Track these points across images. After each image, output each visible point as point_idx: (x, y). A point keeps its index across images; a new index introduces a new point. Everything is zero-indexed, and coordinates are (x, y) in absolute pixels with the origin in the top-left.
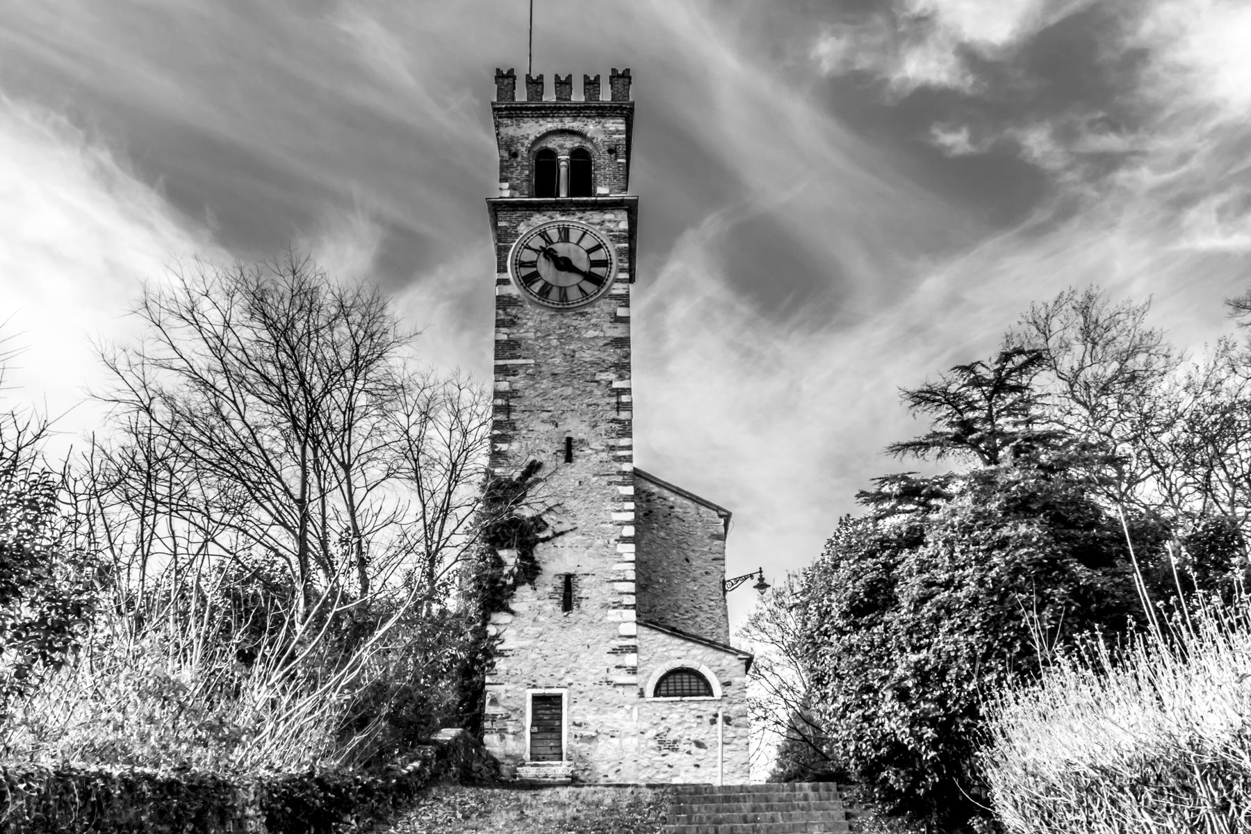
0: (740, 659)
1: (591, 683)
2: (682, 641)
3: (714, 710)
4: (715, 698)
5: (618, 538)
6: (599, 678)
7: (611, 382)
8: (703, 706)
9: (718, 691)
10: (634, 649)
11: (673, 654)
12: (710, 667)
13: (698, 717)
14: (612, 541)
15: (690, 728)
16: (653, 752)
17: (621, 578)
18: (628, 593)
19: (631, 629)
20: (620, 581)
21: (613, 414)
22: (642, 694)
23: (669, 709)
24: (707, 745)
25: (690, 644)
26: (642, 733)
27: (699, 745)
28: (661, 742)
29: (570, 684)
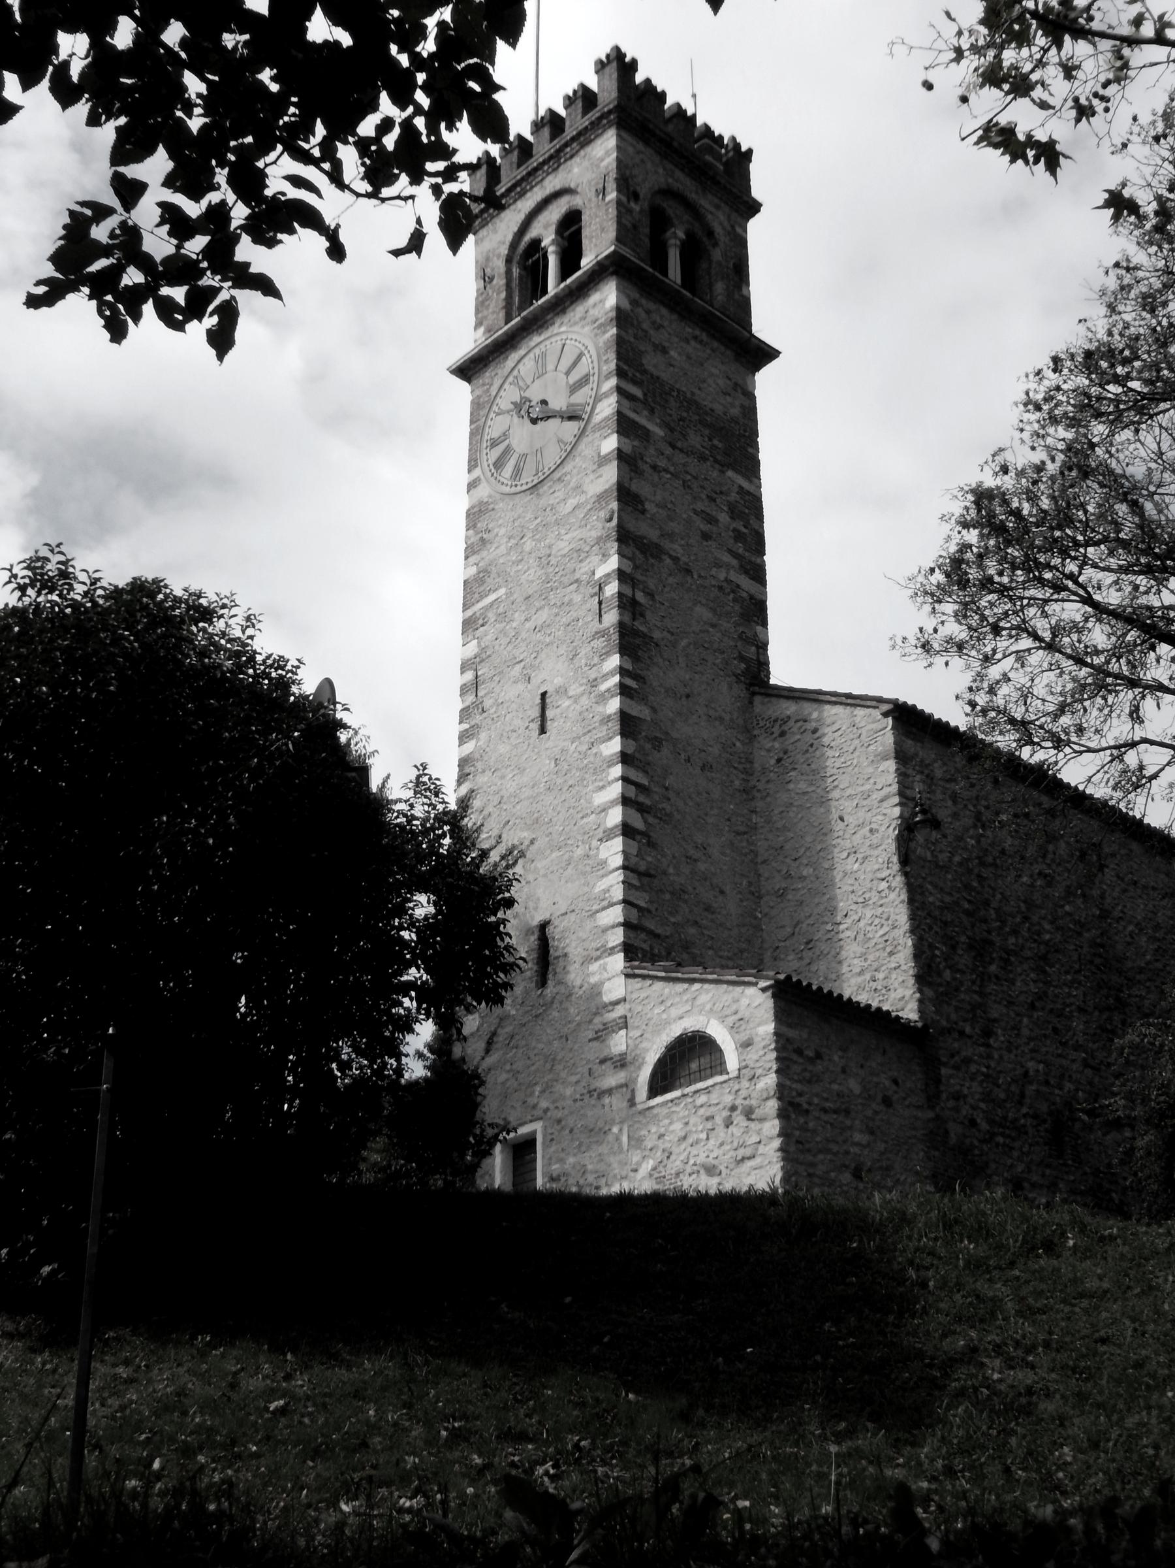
0: (764, 990)
1: (570, 1102)
2: (686, 986)
3: (728, 1099)
4: (731, 1076)
5: (601, 835)
6: (580, 1089)
8: (714, 1098)
9: (732, 1061)
11: (674, 1012)
12: (722, 1019)
13: (707, 1119)
14: (595, 843)
15: (697, 1142)
17: (605, 903)
18: (613, 927)
20: (604, 909)
24: (722, 1168)
25: (697, 986)
29: (546, 1110)
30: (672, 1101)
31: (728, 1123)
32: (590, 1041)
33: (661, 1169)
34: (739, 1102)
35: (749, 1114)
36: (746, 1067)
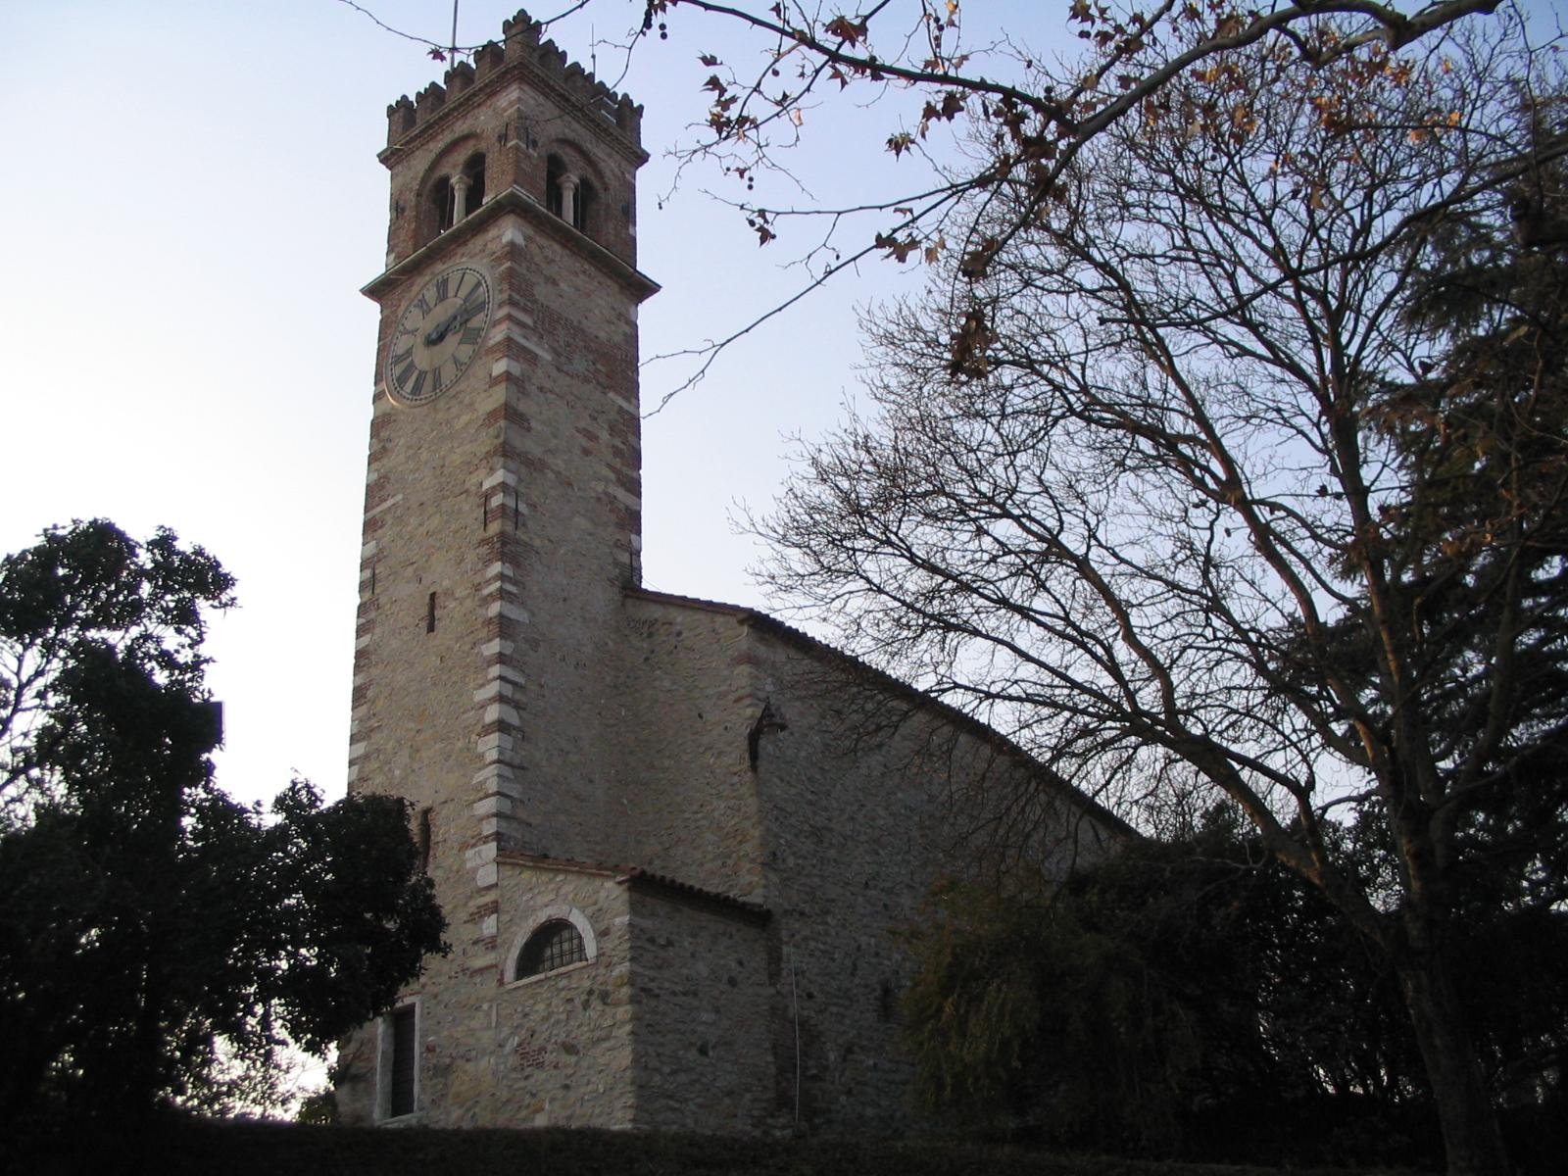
3: (587, 984)
7: (481, 485)
10: (494, 908)
16: (514, 1075)
17: (481, 794)
19: (488, 875)
20: (481, 799)
21: (480, 534)
22: (501, 982)
23: (532, 997)
26: (500, 1046)
27: (570, 1049)
28: (524, 1056)
30: (536, 983)
31: (586, 1005)
32: (465, 922)
33: (525, 1045)
34: (595, 987)
35: (604, 997)
36: (603, 954)
